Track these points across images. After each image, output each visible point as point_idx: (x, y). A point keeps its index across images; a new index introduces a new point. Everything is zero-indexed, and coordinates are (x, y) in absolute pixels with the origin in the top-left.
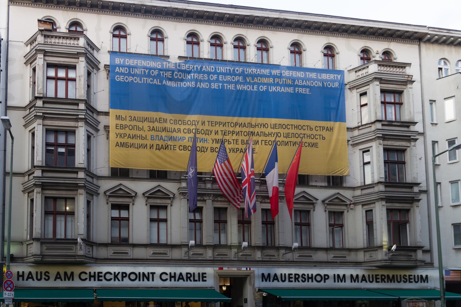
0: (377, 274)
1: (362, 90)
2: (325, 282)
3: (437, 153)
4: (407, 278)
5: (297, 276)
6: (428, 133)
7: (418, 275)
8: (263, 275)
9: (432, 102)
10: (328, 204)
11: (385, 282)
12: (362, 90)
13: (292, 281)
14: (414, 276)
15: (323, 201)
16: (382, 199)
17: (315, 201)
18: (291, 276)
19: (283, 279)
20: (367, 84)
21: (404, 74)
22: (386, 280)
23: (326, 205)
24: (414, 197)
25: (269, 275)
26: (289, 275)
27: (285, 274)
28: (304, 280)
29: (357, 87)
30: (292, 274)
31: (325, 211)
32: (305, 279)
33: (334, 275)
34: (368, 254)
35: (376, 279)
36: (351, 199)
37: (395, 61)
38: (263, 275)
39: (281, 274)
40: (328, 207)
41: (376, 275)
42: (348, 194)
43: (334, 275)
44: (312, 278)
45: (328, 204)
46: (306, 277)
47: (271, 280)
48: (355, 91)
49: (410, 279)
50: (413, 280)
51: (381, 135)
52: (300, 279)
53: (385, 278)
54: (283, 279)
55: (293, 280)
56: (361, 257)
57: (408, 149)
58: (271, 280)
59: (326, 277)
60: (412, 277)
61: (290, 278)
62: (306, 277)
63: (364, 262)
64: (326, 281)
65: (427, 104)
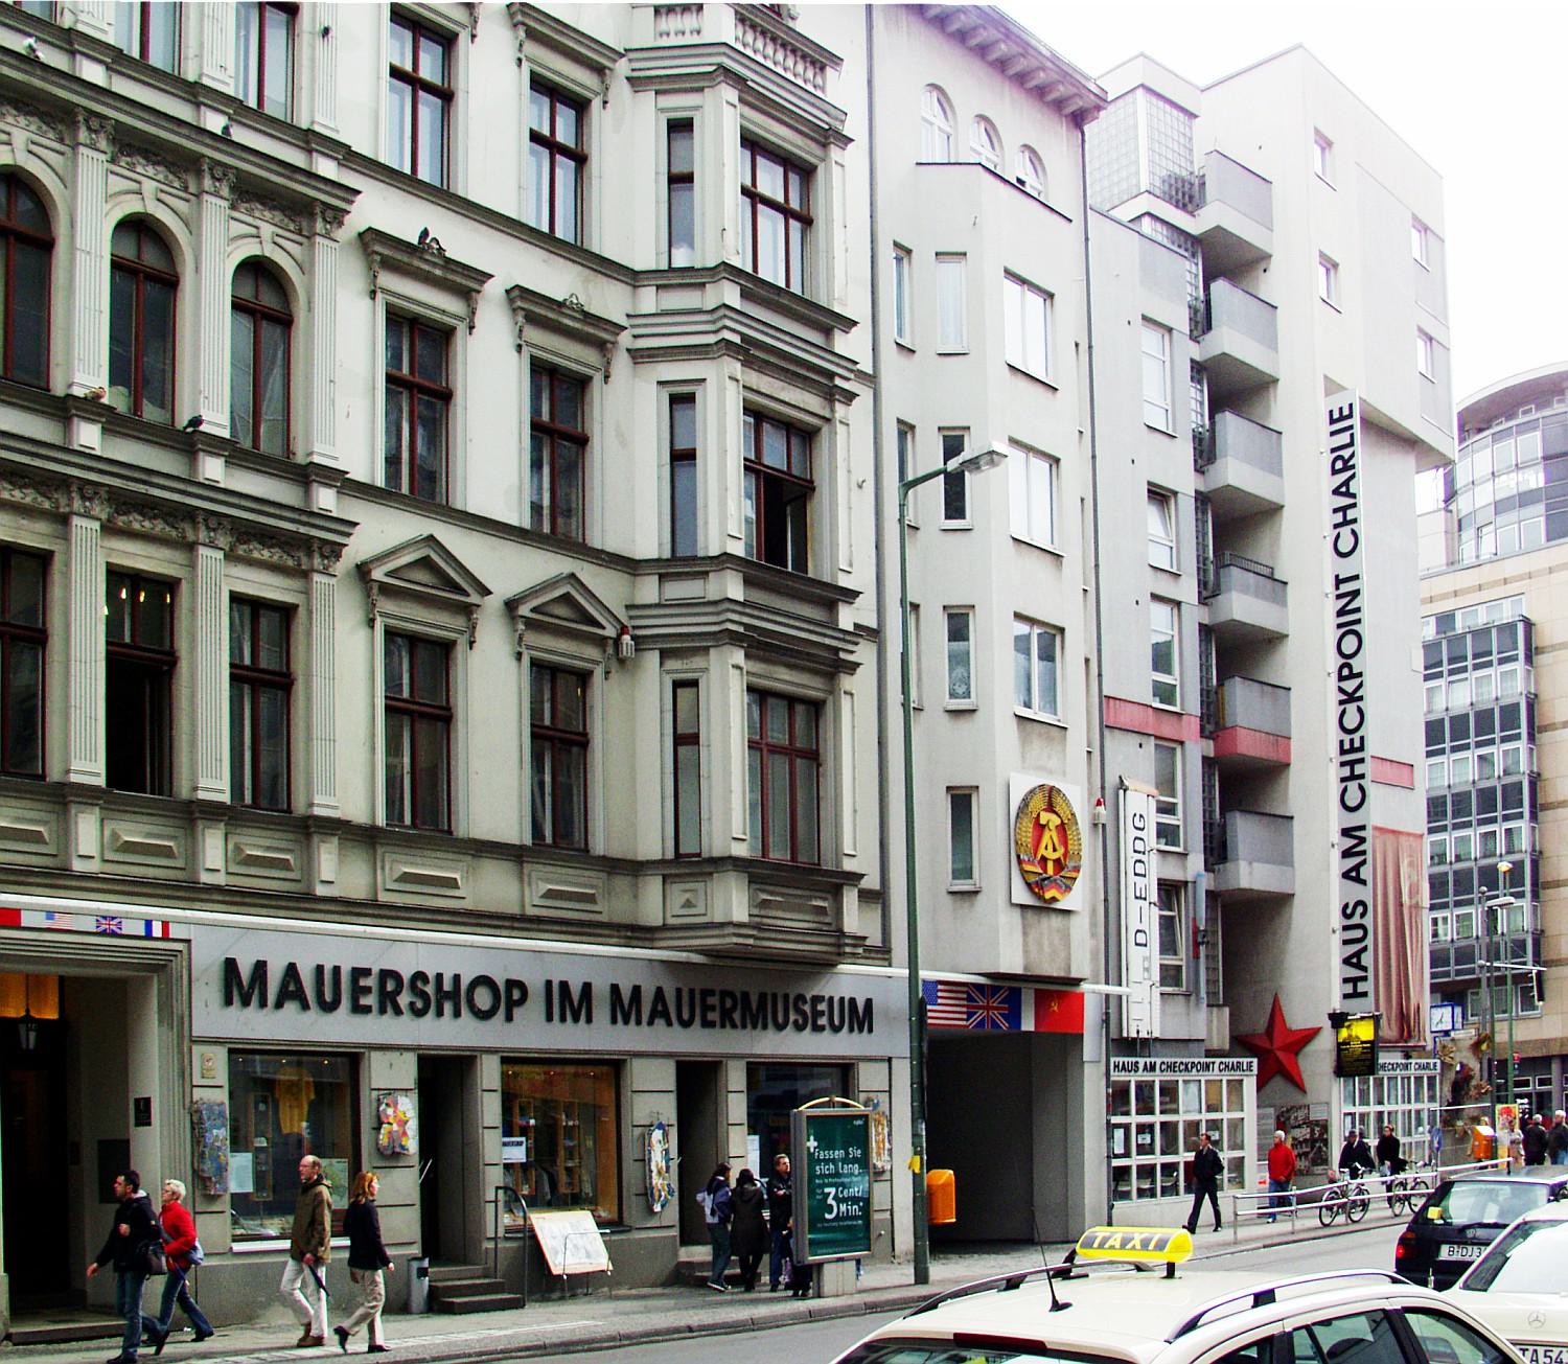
0: (709, 985)
1: (679, 103)
2: (509, 1018)
3: (910, 477)
4: (807, 1008)
5: (390, 986)
6: (887, 380)
7: (842, 999)
8: (230, 966)
9: (903, 252)
10: (530, 624)
11: (734, 1026)
12: (679, 103)
13: (367, 1010)
14: (831, 999)
15: (511, 605)
16: (734, 639)
17: (474, 598)
18: (363, 982)
19: (328, 997)
20: (695, 83)
21: (819, 93)
22: (737, 1016)
23: (521, 627)
24: (836, 650)
25: (260, 968)
26: (359, 973)
27: (337, 970)
28: (419, 1005)
29: (665, 85)
30: (367, 972)
31: (519, 656)
32: (424, 995)
33: (549, 983)
34: (678, 893)
35: (706, 1008)
36: (623, 616)
37: (791, 24)
38: (230, 966)
39: (320, 969)
40: (532, 638)
41: (706, 993)
42: (606, 586)
43: (549, 983)
44: (454, 995)
45: (530, 624)
46: (430, 989)
47: (271, 997)
48: (648, 97)
49: (817, 1014)
50: (823, 1021)
51: (737, 339)
52: (404, 999)
53: (734, 1008)
54: (328, 997)
55: (370, 1000)
56: (652, 903)
57: (825, 429)
58: (271, 997)
59: (516, 995)
60: (822, 1007)
61: (358, 991)
62: (430, 989)
63: (665, 927)
64: (516, 1012)
65: (887, 255)
